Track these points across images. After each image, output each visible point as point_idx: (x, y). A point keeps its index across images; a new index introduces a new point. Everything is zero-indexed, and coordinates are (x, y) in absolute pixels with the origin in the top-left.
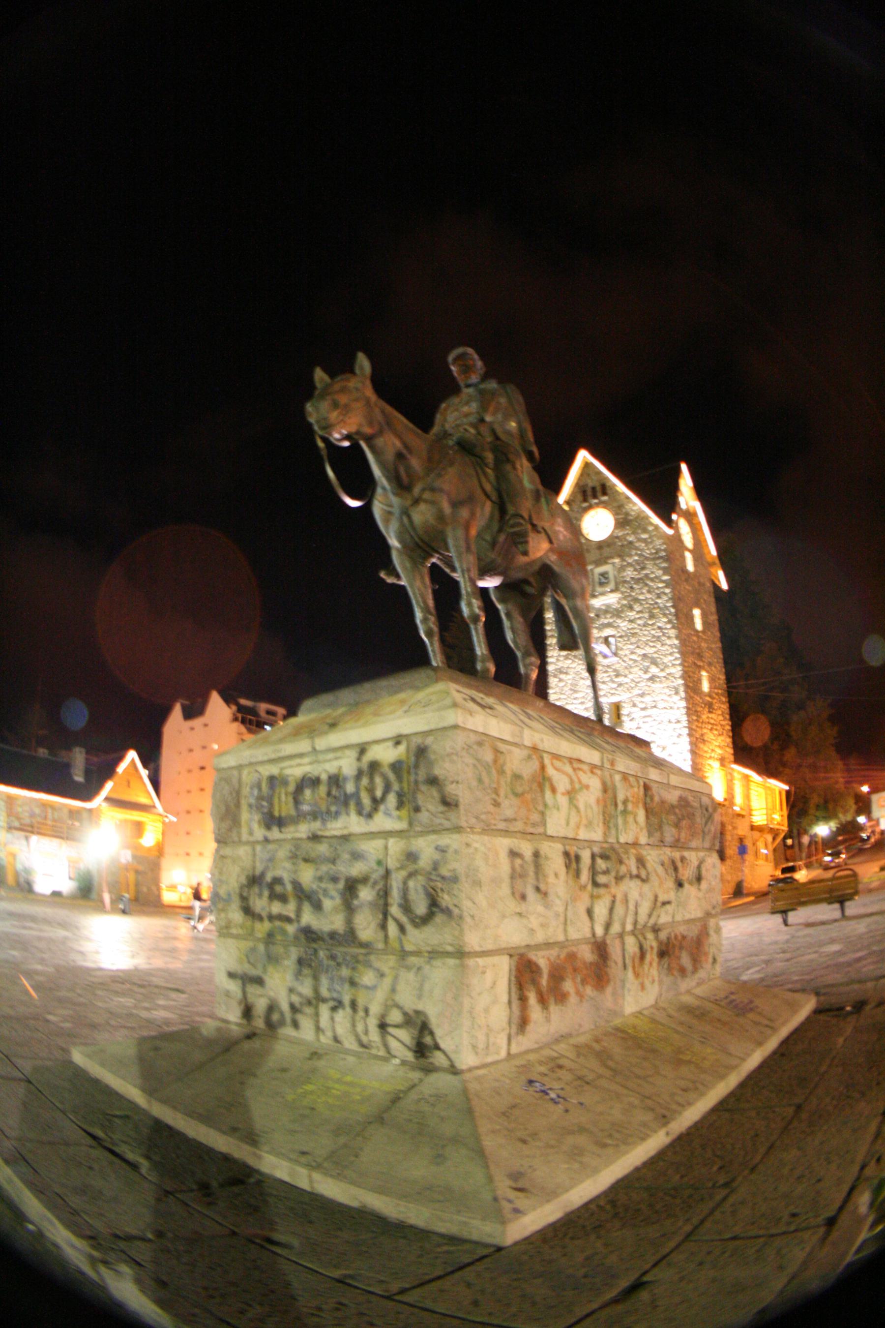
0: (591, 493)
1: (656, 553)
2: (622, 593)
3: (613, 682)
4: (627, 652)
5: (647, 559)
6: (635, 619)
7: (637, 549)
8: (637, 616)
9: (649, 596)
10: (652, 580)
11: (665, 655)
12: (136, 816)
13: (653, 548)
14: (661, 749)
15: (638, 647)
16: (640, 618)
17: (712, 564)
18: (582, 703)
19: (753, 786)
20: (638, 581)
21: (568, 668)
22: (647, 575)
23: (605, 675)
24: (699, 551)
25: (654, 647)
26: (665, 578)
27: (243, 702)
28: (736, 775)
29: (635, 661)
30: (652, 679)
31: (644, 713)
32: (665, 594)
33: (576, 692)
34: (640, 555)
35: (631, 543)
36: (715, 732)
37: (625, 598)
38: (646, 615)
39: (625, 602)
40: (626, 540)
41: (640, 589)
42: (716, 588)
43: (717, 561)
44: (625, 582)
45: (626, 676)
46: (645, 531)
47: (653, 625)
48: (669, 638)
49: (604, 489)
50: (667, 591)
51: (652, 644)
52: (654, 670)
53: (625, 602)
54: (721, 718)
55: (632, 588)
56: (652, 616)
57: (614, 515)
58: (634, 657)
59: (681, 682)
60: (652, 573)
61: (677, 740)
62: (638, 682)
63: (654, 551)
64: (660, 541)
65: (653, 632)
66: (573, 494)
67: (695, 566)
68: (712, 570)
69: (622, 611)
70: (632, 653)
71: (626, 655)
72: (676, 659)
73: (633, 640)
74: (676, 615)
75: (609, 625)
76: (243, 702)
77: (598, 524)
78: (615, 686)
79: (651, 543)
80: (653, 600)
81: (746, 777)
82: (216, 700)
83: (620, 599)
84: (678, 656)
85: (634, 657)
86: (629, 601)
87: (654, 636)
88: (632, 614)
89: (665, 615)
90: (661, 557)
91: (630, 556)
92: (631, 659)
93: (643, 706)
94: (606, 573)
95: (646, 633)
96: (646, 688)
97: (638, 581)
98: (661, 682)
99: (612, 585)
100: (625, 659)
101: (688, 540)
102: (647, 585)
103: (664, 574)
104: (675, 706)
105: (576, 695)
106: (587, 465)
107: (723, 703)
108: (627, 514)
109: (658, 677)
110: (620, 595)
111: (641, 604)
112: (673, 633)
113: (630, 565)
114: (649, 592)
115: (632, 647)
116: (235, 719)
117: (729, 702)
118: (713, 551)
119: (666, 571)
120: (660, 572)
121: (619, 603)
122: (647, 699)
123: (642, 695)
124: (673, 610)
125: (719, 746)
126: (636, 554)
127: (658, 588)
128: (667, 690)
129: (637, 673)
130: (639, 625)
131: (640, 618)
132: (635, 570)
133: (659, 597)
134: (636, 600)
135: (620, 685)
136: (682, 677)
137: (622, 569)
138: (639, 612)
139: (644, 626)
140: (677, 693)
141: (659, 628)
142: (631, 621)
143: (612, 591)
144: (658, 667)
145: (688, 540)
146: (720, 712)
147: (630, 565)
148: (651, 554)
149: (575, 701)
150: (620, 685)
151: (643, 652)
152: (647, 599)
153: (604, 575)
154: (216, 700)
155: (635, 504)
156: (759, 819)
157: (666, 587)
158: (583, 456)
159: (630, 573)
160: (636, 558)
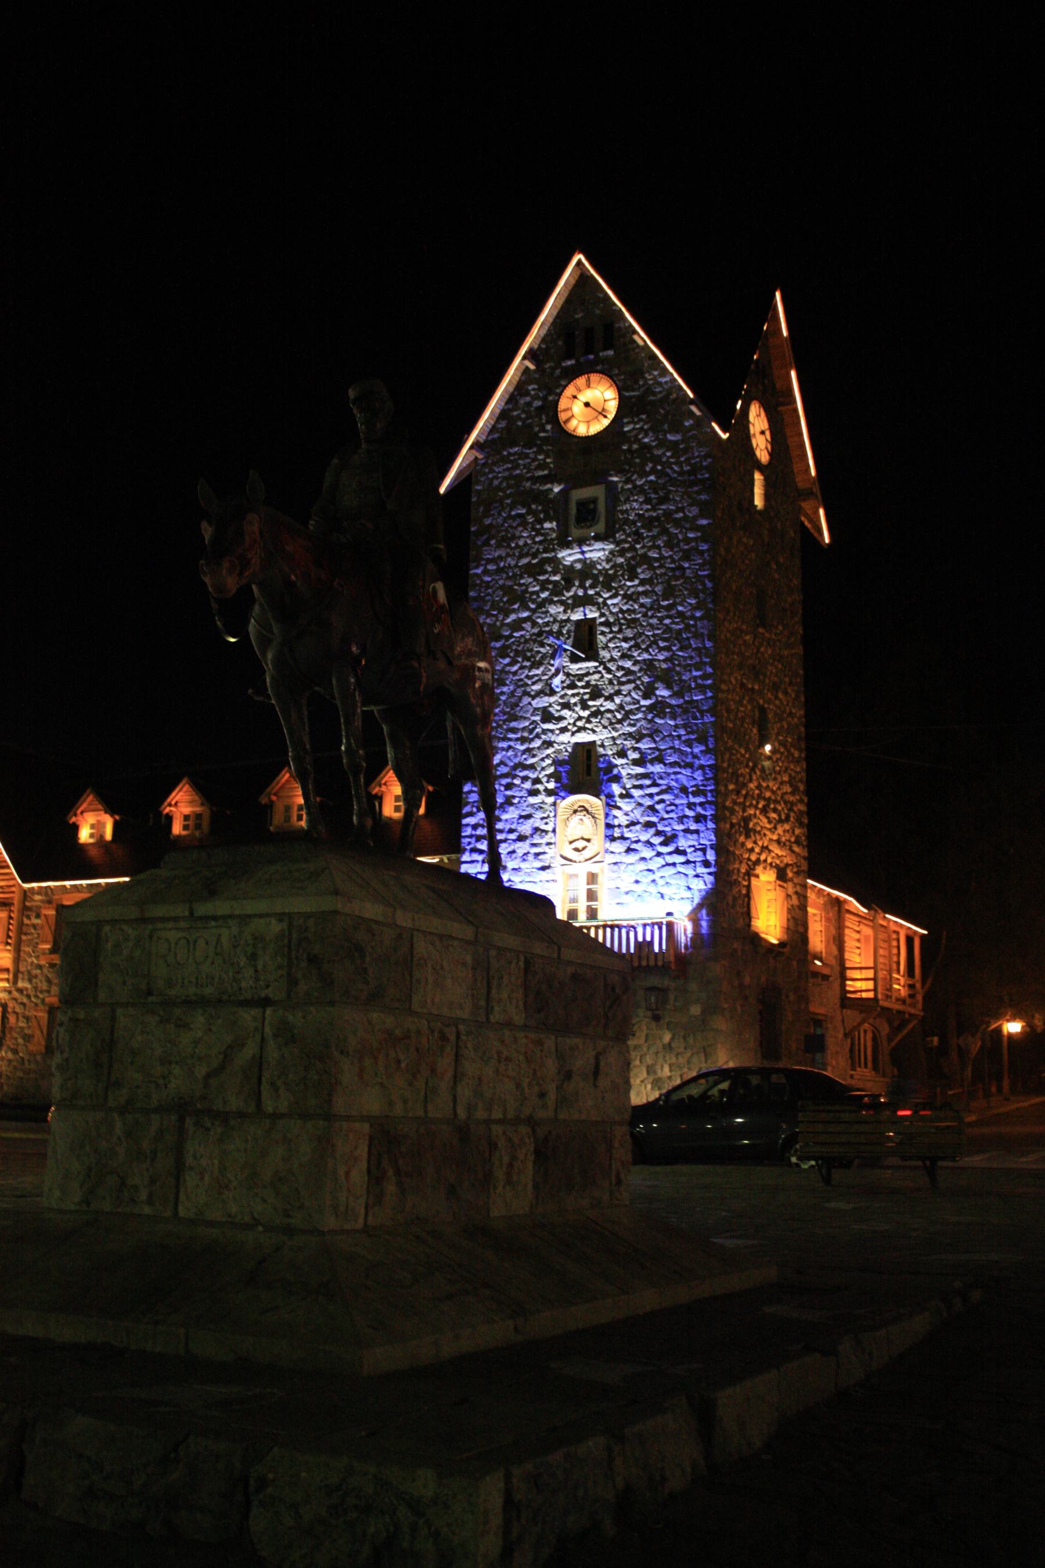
0: (584, 345)
1: (693, 472)
2: (618, 543)
3: (585, 707)
4: (616, 654)
5: (672, 481)
6: (639, 594)
7: (657, 460)
8: (640, 589)
9: (666, 553)
10: (677, 523)
11: (688, 668)
13: (687, 460)
14: (661, 839)
15: (637, 646)
16: (645, 593)
17: (808, 494)
18: (523, 740)
19: (850, 922)
20: (649, 523)
21: (503, 671)
22: (668, 514)
23: (570, 692)
24: (781, 466)
25: (667, 649)
26: (704, 522)
28: (811, 896)
29: (628, 672)
30: (659, 708)
31: (640, 770)
32: (702, 553)
33: (516, 718)
34: (660, 474)
35: (646, 447)
36: (774, 815)
37: (622, 553)
38: (658, 589)
39: (620, 560)
40: (638, 440)
41: (654, 538)
43: (816, 489)
44: (626, 521)
45: (610, 698)
46: (676, 428)
47: (668, 608)
48: (696, 636)
49: (611, 332)
50: (704, 547)
51: (662, 644)
52: (663, 692)
53: (620, 560)
54: (787, 789)
55: (637, 533)
57: (620, 391)
58: (628, 664)
59: (708, 719)
60: (682, 509)
61: (693, 826)
62: (631, 712)
63: (686, 468)
64: (703, 451)
65: (667, 621)
66: (546, 339)
67: (767, 497)
68: (807, 506)
69: (613, 578)
70: (624, 656)
71: (612, 659)
72: (705, 677)
73: (629, 633)
77: (590, 406)
78: (585, 714)
79: (685, 451)
80: (673, 561)
81: (838, 902)
83: (612, 552)
84: (709, 670)
85: (628, 664)
86: (628, 560)
87: (668, 630)
89: (694, 593)
90: (702, 482)
91: (644, 474)
92: (620, 668)
93: (635, 756)
94: (594, 501)
95: (654, 621)
96: (643, 722)
97: (649, 523)
98: (674, 718)
99: (600, 527)
100: (612, 666)
101: (761, 446)
102: (665, 531)
103: (702, 515)
104: (697, 762)
105: (513, 724)
106: (583, 280)
107: (798, 762)
108: (649, 391)
109: (670, 706)
110: (612, 546)
111: (651, 568)
112: (703, 627)
113: (641, 490)
114: (669, 545)
115: (625, 645)
117: (807, 759)
119: (705, 510)
120: (694, 511)
121: (608, 561)
122: (645, 745)
123: (638, 737)
124: (709, 585)
125: (778, 842)
126: (653, 471)
127: (687, 541)
128: (682, 732)
129: (630, 695)
130: (642, 605)
131: (645, 593)
132: (648, 501)
133: (687, 556)
134: (645, 559)
135: (597, 713)
136: (712, 711)
138: (643, 582)
139: (651, 608)
140: (702, 740)
141: (680, 614)
142: (627, 597)
143: (598, 538)
144: (669, 687)
145: (761, 446)
146: (786, 778)
147: (641, 490)
148: (681, 473)
149: (511, 736)
150: (597, 713)
151: (646, 656)
152: (662, 558)
155: (664, 371)
156: (860, 985)
157: (703, 539)
160: (652, 478)
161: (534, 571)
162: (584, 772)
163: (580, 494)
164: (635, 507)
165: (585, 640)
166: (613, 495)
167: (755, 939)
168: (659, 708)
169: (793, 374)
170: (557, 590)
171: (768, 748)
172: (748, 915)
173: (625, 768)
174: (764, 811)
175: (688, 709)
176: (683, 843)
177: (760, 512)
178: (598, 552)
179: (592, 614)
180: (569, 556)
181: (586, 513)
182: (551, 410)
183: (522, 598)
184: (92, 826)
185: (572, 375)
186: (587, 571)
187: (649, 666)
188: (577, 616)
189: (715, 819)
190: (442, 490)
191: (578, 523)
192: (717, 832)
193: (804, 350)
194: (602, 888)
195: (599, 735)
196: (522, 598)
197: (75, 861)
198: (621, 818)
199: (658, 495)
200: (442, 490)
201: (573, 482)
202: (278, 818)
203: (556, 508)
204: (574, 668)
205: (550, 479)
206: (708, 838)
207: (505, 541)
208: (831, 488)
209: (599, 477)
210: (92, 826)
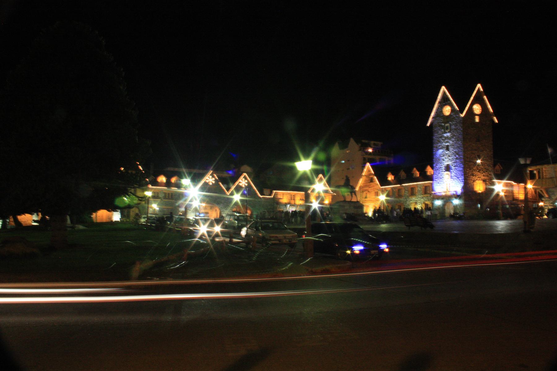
0: (445, 101)
27: (363, 141)
30: (457, 159)
42: (493, 121)
56: (458, 140)
67: (480, 119)
75: (447, 142)
76: (363, 141)
77: (447, 110)
82: (352, 141)
88: (453, 139)
97: (455, 129)
99: (449, 130)
116: (360, 150)
118: (491, 110)
129: (453, 157)
154: (352, 141)
158: (443, 88)
161: (441, 137)
162: (448, 168)
163: (447, 125)
164: (453, 127)
165: (447, 149)
166: (450, 125)
167: (475, 193)
168: (457, 159)
169: (485, 97)
171: (479, 161)
172: (473, 188)
173: (453, 168)
174: (479, 172)
175: (460, 159)
177: (477, 123)
178: (448, 134)
180: (445, 135)
181: (447, 128)
182: (442, 112)
183: (440, 142)
184: (390, 178)
185: (446, 105)
186: (447, 138)
187: (455, 152)
188: (447, 144)
189: (464, 175)
190: (428, 125)
193: (486, 92)
195: (450, 163)
196: (440, 142)
197: (389, 183)
198: (453, 175)
199: (456, 125)
200: (428, 125)
201: (445, 123)
202: (414, 175)
203: (443, 127)
204: (447, 152)
205: (443, 123)
206: (463, 178)
208: (496, 113)
209: (447, 122)
210: (390, 178)
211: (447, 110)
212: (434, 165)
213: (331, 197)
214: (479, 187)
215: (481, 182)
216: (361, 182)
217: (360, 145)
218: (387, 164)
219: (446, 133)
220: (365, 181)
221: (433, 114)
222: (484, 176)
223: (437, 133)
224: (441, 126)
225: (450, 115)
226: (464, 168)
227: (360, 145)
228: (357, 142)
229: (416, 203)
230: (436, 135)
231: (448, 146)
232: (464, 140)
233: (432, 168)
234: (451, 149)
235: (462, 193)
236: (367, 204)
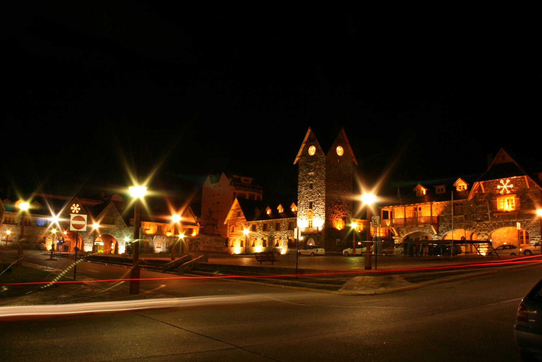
12: (190, 227)
27: (234, 176)
30: (319, 197)
74: (326, 180)
75: (311, 181)
97: (319, 169)
116: (231, 184)
119: (325, 167)
129: (316, 195)
134: (318, 174)
137: (315, 165)
153: (312, 166)
159: (317, 166)
161: (305, 176)
163: (311, 164)
164: (317, 166)
170: (308, 179)
174: (339, 210)
176: (322, 216)
178: (313, 173)
179: (311, 182)
180: (310, 174)
182: (307, 151)
186: (311, 176)
190: (295, 163)
191: (310, 169)
192: (326, 215)
194: (313, 222)
196: (304, 180)
200: (295, 163)
201: (311, 162)
203: (307, 166)
205: (308, 162)
207: (302, 171)
211: (312, 151)
212: (299, 202)
213: (198, 229)
214: (339, 225)
215: (340, 220)
216: (229, 217)
217: (231, 179)
218: (256, 199)
219: (311, 172)
220: (233, 215)
221: (299, 154)
222: (343, 214)
223: (302, 171)
224: (306, 165)
225: (314, 155)
226: (326, 206)
227: (231, 179)
228: (228, 176)
229: (280, 238)
230: (301, 173)
231: (311, 184)
232: (327, 181)
233: (297, 205)
234: (314, 187)
235: (323, 230)
236: (234, 238)
